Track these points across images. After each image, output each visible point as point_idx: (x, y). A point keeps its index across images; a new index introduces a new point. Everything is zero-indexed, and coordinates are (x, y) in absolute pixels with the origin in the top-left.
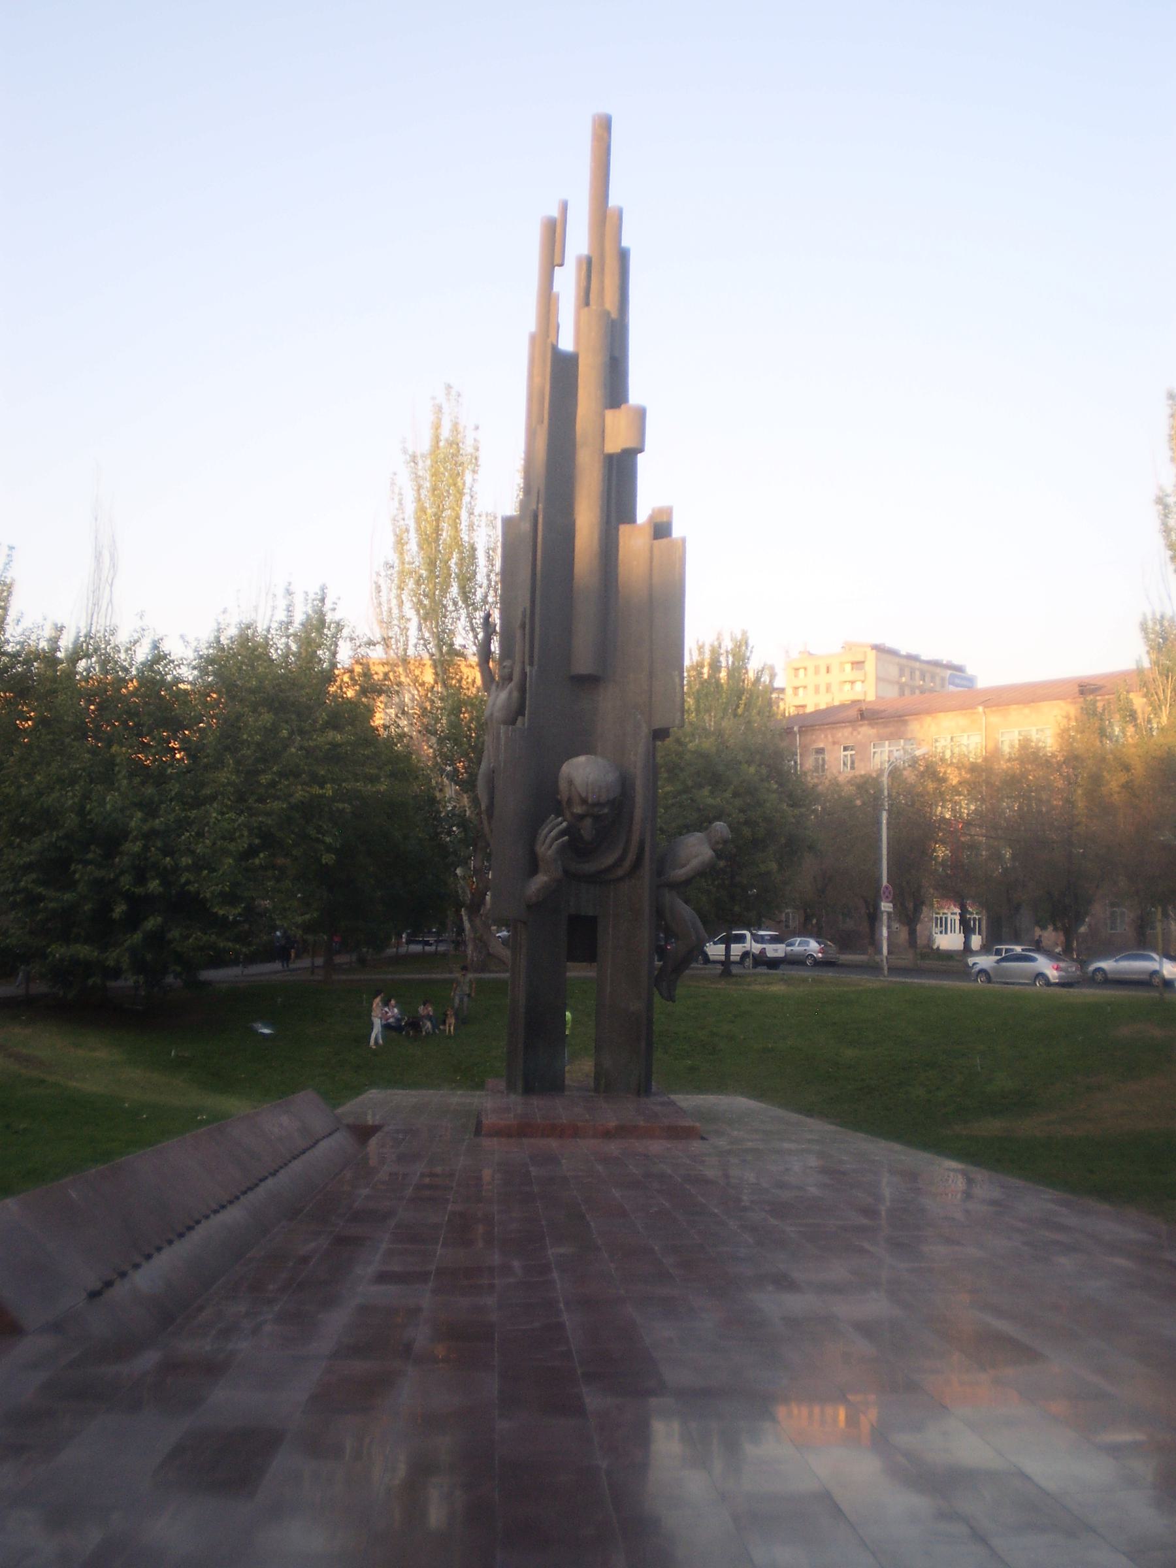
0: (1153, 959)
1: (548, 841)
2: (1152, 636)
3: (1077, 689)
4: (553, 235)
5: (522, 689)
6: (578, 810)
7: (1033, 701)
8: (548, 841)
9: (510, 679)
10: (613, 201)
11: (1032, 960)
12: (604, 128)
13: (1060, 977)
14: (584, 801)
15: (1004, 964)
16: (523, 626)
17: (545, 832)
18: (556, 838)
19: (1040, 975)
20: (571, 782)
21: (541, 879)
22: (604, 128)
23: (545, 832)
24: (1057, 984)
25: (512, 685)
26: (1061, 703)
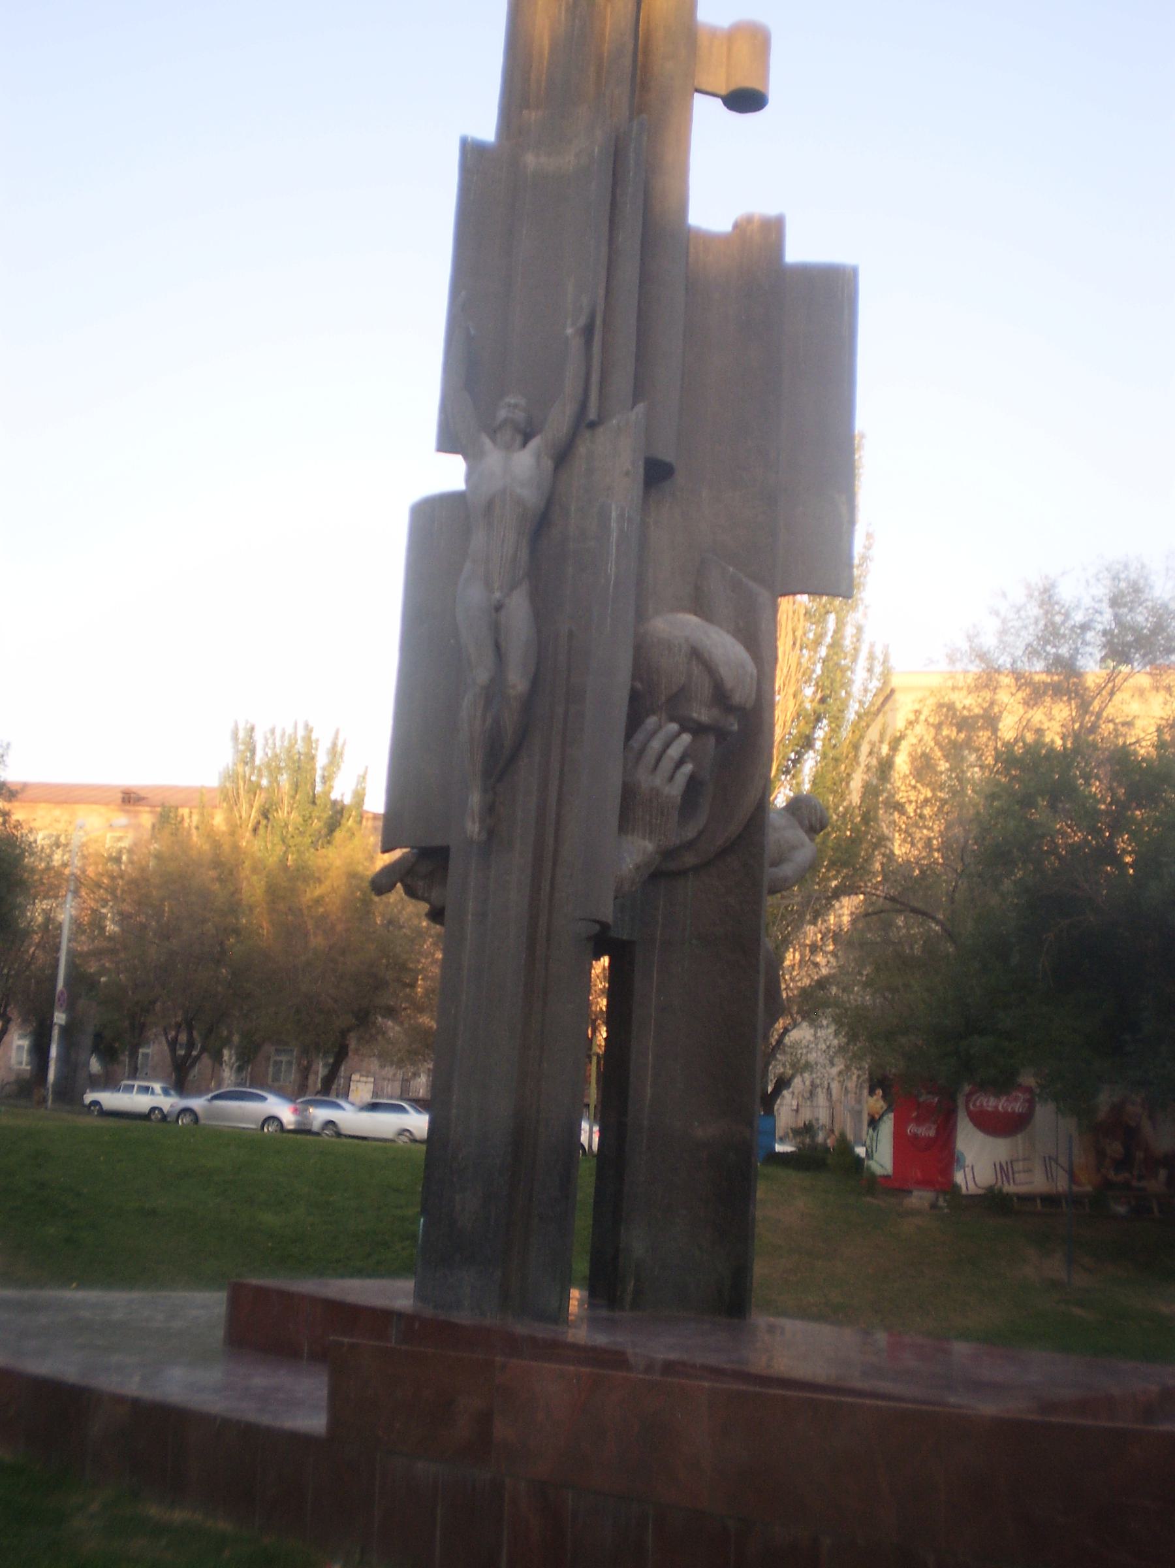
0: (339, 1106)
1: (667, 765)
2: (242, 747)
3: (120, 795)
5: (562, 456)
6: (703, 714)
7: (65, 802)
8: (667, 765)
11: (264, 1099)
13: (298, 1123)
17: (656, 744)
18: (680, 763)
20: (696, 654)
23: (656, 744)
24: (290, 1131)
25: (534, 443)
26: (103, 809)
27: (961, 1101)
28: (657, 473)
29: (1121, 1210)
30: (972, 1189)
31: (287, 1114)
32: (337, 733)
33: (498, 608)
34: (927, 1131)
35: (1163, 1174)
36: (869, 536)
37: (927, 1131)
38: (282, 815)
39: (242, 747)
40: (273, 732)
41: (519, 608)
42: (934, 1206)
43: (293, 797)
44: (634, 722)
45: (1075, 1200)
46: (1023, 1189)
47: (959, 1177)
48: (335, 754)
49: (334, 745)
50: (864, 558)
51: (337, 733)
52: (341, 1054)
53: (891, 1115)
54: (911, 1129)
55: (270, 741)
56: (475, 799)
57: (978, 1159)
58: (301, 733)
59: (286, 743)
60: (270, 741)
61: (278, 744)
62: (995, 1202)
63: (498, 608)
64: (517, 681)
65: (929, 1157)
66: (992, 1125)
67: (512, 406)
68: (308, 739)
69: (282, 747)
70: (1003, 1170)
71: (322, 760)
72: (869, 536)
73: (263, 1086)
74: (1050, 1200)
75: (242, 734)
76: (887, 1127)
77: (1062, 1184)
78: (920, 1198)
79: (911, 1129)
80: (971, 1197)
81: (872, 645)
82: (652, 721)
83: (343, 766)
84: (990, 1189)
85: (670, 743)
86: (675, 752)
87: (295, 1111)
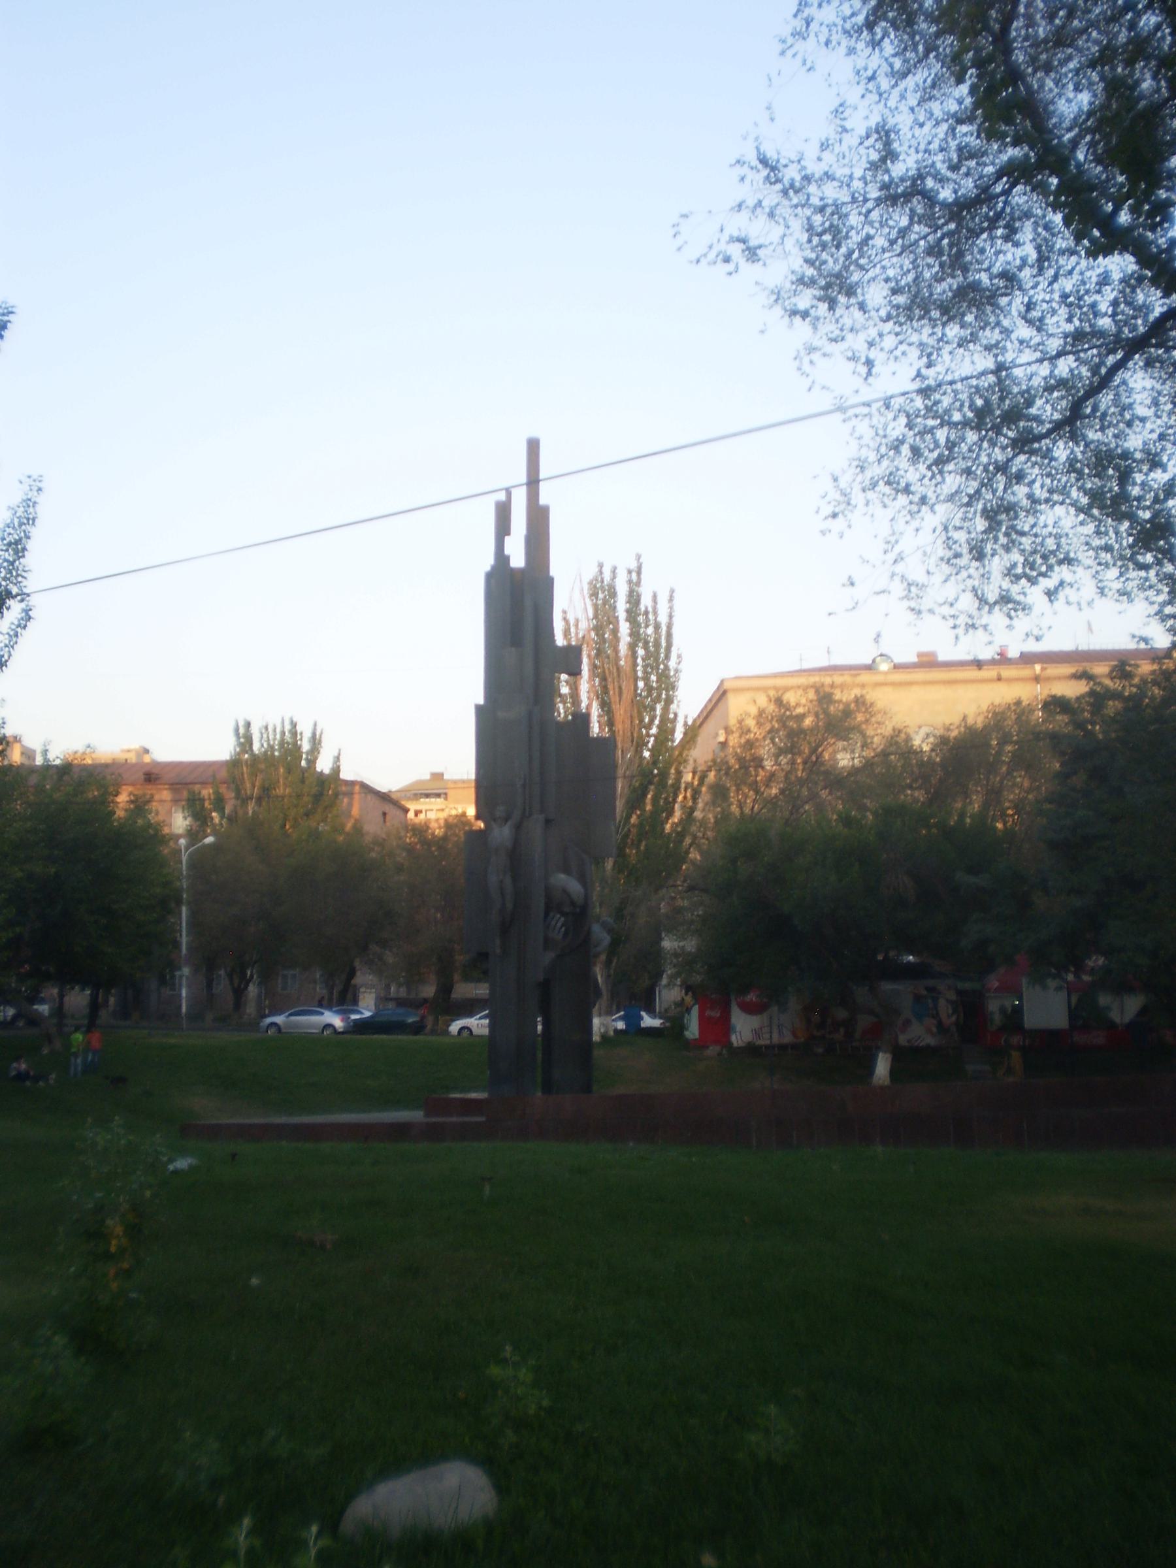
2: (242, 740)
4: (503, 514)
5: (518, 827)
6: (567, 909)
9: (506, 820)
10: (543, 501)
12: (533, 447)
14: (573, 903)
15: (293, 1018)
16: (524, 786)
19: (329, 1026)
20: (565, 891)
21: (548, 957)
22: (533, 447)
23: (553, 923)
24: (342, 1033)
25: (509, 823)
27: (733, 998)
28: (548, 822)
29: (820, 1050)
30: (741, 1044)
31: (337, 1022)
32: (315, 725)
33: (501, 882)
34: (715, 1014)
35: (842, 1030)
36: (679, 656)
37: (715, 1014)
38: (280, 791)
39: (242, 740)
40: (266, 728)
41: (508, 881)
42: (720, 1054)
43: (286, 778)
44: (546, 914)
45: (794, 1046)
46: (768, 1042)
47: (733, 1038)
48: (316, 742)
49: (314, 734)
50: (677, 671)
51: (315, 725)
52: (352, 974)
53: (697, 1007)
54: (708, 1013)
55: (265, 736)
56: (498, 942)
57: (744, 1028)
58: (288, 727)
59: (278, 737)
60: (265, 736)
61: (271, 737)
62: (751, 1050)
63: (501, 882)
64: (509, 906)
65: (717, 1028)
66: (748, 1009)
67: (500, 811)
68: (294, 733)
69: (275, 739)
70: (757, 1033)
71: (306, 746)
72: (679, 656)
73: (320, 1005)
74: (783, 1047)
75: (242, 731)
76: (695, 1012)
77: (788, 1039)
78: (712, 1050)
79: (708, 1013)
80: (739, 1048)
81: (686, 717)
82: (551, 914)
83: (322, 750)
84: (749, 1043)
85: (558, 921)
86: (559, 924)
87: (342, 1020)
